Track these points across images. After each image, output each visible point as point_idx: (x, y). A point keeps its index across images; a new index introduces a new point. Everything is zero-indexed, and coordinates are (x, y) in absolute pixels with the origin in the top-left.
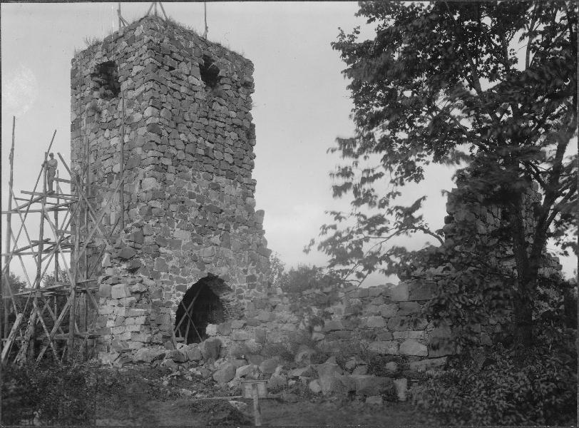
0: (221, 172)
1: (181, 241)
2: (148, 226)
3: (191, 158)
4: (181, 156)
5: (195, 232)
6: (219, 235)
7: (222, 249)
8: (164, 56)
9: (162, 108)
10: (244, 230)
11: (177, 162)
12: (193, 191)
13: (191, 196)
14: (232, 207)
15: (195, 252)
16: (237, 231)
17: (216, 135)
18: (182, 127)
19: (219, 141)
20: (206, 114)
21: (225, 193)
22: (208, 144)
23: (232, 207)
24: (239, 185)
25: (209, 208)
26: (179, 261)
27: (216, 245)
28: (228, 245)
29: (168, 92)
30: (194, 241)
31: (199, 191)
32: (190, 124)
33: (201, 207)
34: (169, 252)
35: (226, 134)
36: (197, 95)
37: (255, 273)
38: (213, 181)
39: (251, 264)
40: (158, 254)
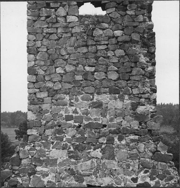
0: (103, 90)
1: (57, 159)
2: (25, 151)
3: (68, 86)
4: (58, 86)
5: (72, 149)
6: (100, 149)
7: (103, 161)
8: (39, 10)
9: (38, 52)
10: (132, 141)
11: (52, 93)
12: (70, 114)
13: (69, 118)
14: (116, 121)
15: (73, 167)
16: (123, 142)
17: (97, 58)
18: (58, 63)
19: (100, 62)
20: (84, 43)
21: (109, 108)
22: (88, 68)
23: (116, 121)
24: (126, 97)
25: (89, 126)
26: (55, 177)
27: (97, 158)
28: (112, 157)
29: (44, 37)
30: (70, 157)
31: (77, 113)
32: (67, 57)
33: (80, 126)
34: (45, 169)
35: (110, 54)
36: (74, 31)
37: (148, 180)
38: (95, 100)
39: (143, 172)
40: (34, 172)
